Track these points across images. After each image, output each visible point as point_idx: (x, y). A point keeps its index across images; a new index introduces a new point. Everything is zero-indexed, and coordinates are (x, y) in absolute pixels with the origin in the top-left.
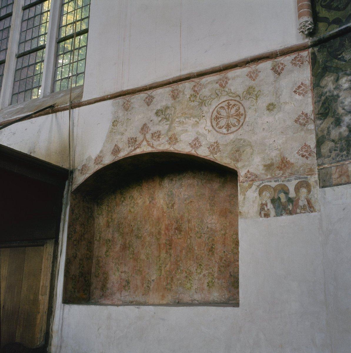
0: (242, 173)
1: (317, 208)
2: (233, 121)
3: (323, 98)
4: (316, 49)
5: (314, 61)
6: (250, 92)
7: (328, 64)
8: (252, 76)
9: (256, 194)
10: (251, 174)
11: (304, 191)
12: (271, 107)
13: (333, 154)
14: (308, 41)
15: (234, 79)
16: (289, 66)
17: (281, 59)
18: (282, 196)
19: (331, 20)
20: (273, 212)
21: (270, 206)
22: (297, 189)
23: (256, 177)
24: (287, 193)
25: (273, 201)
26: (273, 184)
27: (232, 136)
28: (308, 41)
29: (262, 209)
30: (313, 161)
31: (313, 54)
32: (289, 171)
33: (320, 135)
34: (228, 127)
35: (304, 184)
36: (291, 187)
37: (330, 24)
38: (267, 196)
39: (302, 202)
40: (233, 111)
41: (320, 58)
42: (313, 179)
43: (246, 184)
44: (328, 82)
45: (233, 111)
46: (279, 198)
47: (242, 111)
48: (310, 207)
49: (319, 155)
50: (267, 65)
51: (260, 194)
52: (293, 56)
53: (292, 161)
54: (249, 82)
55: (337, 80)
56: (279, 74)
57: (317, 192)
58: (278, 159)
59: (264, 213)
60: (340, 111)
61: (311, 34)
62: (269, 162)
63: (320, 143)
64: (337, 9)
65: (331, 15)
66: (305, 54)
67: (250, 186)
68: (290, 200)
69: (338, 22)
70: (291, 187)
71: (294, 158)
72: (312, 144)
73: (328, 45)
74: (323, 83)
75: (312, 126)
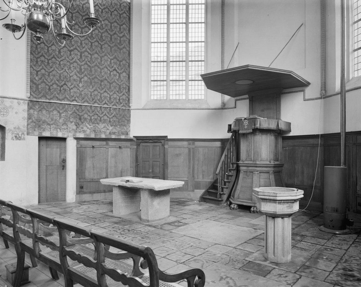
0: (7, 128)
1: (26, 139)
2: (5, 114)
3: (30, 115)
4: (29, 102)
5: (28, 104)
6: (11, 107)
7: (32, 107)
8: (12, 102)
9: (11, 134)
10: (10, 129)
11: (23, 135)
12: (16, 113)
13: (31, 128)
14: (28, 99)
15: (6, 101)
16: (22, 103)
17: (19, 101)
18: (18, 136)
19: (34, 96)
20: (15, 139)
21: (14, 137)
22: (21, 135)
23: (11, 130)
24: (19, 135)
25: (15, 137)
26: (16, 133)
27: (5, 118)
28: (28, 99)
29: (12, 138)
30: (26, 129)
31: (28, 102)
32: (20, 130)
33: (28, 123)
34: (3, 115)
35: (23, 134)
36: (20, 134)
37: (34, 97)
38: (14, 135)
39: (22, 138)
40: (5, 111)
41: (30, 104)
42: (25, 133)
43: (8, 131)
44: (32, 111)
45: (5, 111)
46: (17, 136)
47: (8, 111)
48: (24, 139)
49: (27, 127)
50: (16, 101)
51: (12, 134)
52: (23, 101)
53: (21, 128)
54: (11, 104)
55: (34, 112)
56: (19, 105)
57: (26, 136)
58: (17, 127)
59: (12, 139)
60: (34, 119)
61: (29, 98)
62: (15, 127)
63: (28, 125)
64: (36, 94)
65: (35, 95)
66: (26, 102)
67: (9, 132)
68: (19, 137)
69: (36, 98)
70: (20, 134)
71: (21, 127)
72: (26, 125)
73: (32, 102)
74: (30, 111)
75: (26, 120)
